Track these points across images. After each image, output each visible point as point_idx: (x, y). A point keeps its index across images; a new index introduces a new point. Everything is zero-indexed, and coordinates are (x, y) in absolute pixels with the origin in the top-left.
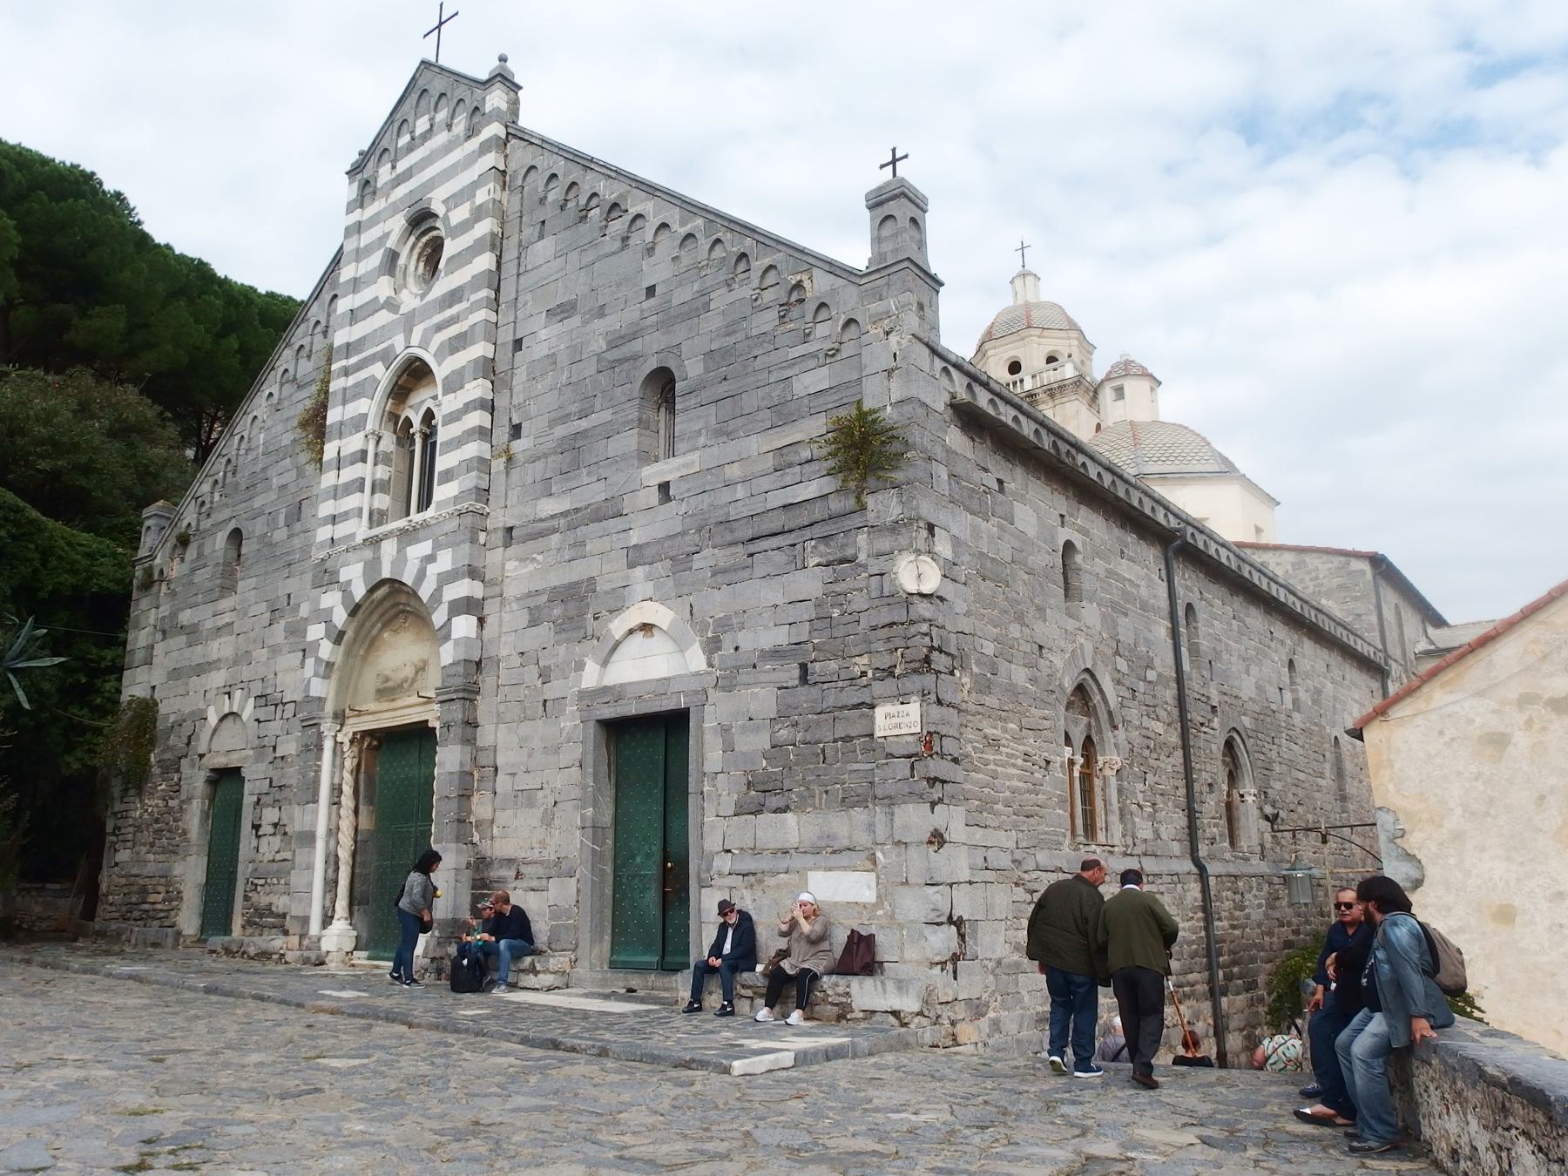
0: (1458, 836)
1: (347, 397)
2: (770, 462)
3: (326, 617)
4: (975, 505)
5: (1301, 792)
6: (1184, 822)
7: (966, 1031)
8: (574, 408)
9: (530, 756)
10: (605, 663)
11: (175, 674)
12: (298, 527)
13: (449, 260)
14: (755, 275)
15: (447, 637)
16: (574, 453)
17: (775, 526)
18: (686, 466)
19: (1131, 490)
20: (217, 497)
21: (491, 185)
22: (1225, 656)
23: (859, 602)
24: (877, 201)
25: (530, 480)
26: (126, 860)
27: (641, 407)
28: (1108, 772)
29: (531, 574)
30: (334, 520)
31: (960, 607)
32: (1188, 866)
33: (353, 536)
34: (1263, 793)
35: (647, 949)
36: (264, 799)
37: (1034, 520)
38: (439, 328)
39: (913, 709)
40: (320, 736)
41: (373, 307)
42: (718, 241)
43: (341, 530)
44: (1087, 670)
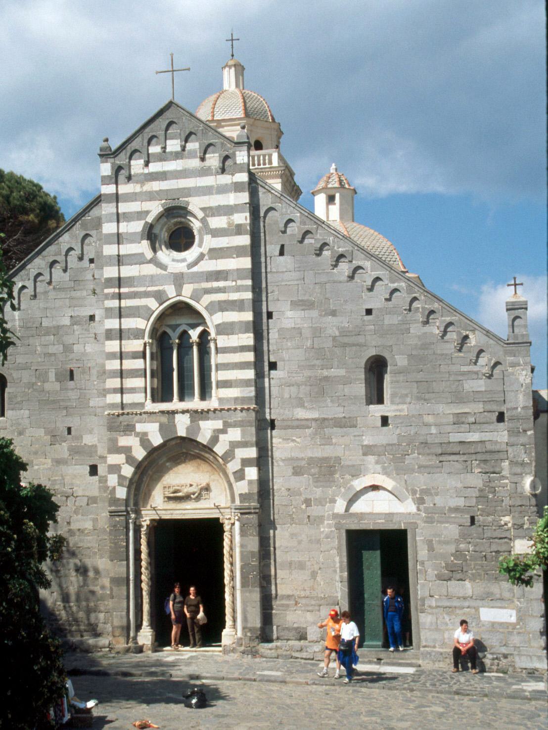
2: (451, 419)
3: (127, 451)
9: (300, 542)
13: (211, 250)
16: (321, 388)
17: (456, 449)
18: (400, 411)
25: (286, 396)
33: (142, 405)
41: (138, 259)
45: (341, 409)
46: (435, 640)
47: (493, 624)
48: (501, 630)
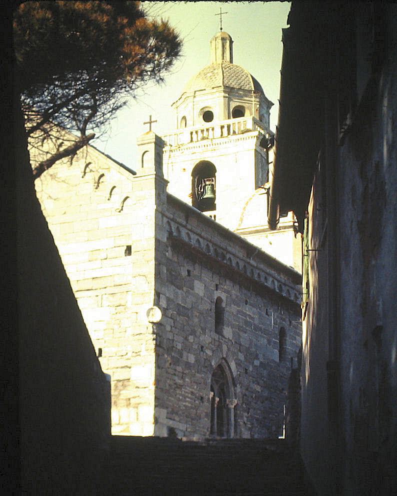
31: (168, 328)
44: (223, 358)
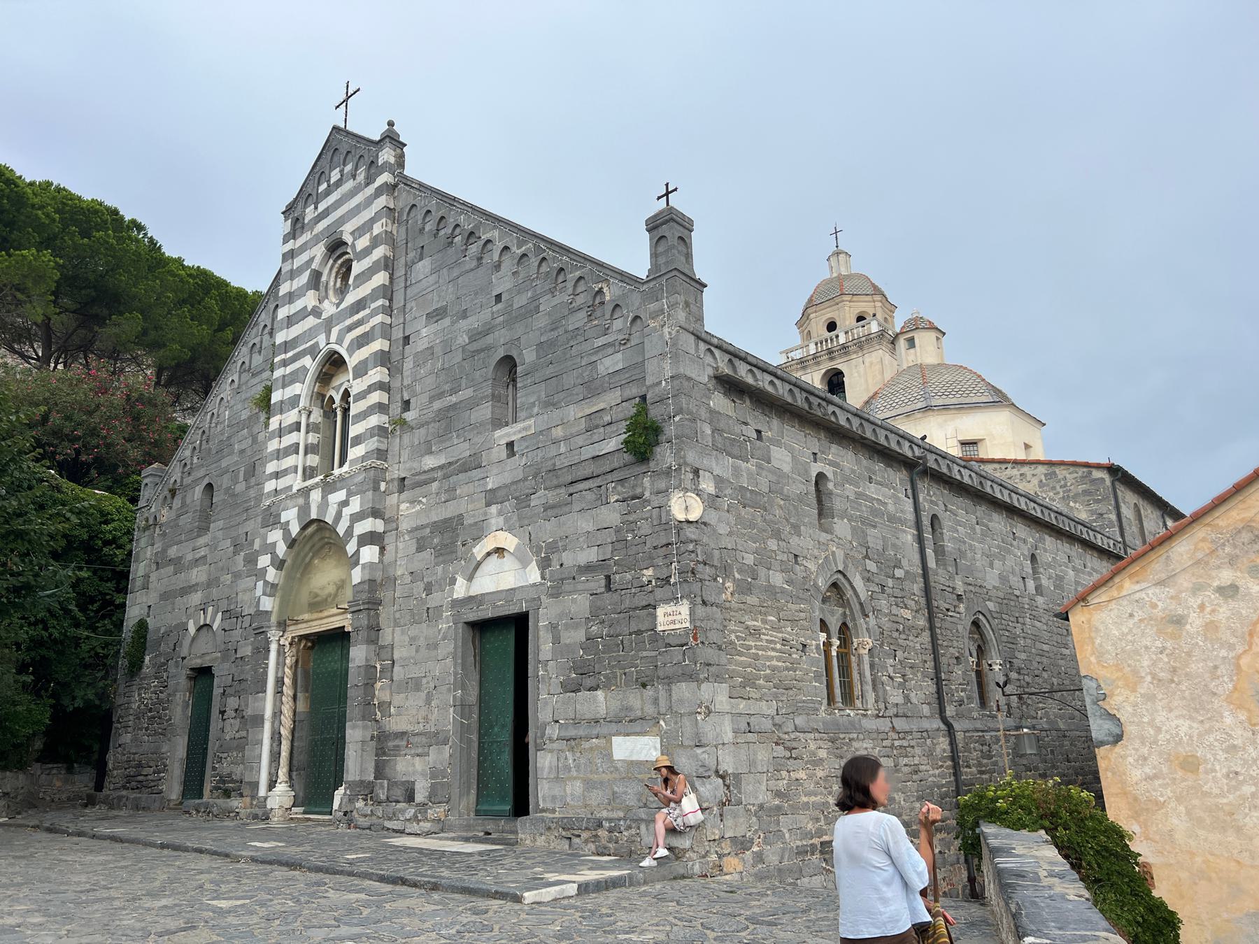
0: (1150, 698)
1: (286, 382)
2: (583, 425)
3: (271, 549)
4: (736, 451)
5: (1045, 660)
6: (933, 689)
7: (732, 863)
8: (447, 387)
10: (470, 578)
11: (166, 596)
12: (253, 481)
13: (356, 277)
14: (570, 285)
15: (357, 563)
16: (448, 422)
17: (587, 473)
18: (525, 429)
19: (878, 430)
20: (195, 460)
21: (384, 220)
22: (969, 554)
23: (645, 528)
24: (655, 225)
26: (127, 741)
27: (493, 386)
28: (862, 651)
29: (418, 512)
30: (277, 475)
31: (723, 529)
32: (937, 723)
34: (1009, 663)
35: (503, 800)
36: (228, 691)
37: (789, 459)
38: (350, 329)
39: (684, 609)
40: (268, 642)
42: (544, 259)
43: (282, 483)
44: (839, 571)
45: (467, 445)
46: (554, 798)
47: (632, 764)
48: (639, 776)
